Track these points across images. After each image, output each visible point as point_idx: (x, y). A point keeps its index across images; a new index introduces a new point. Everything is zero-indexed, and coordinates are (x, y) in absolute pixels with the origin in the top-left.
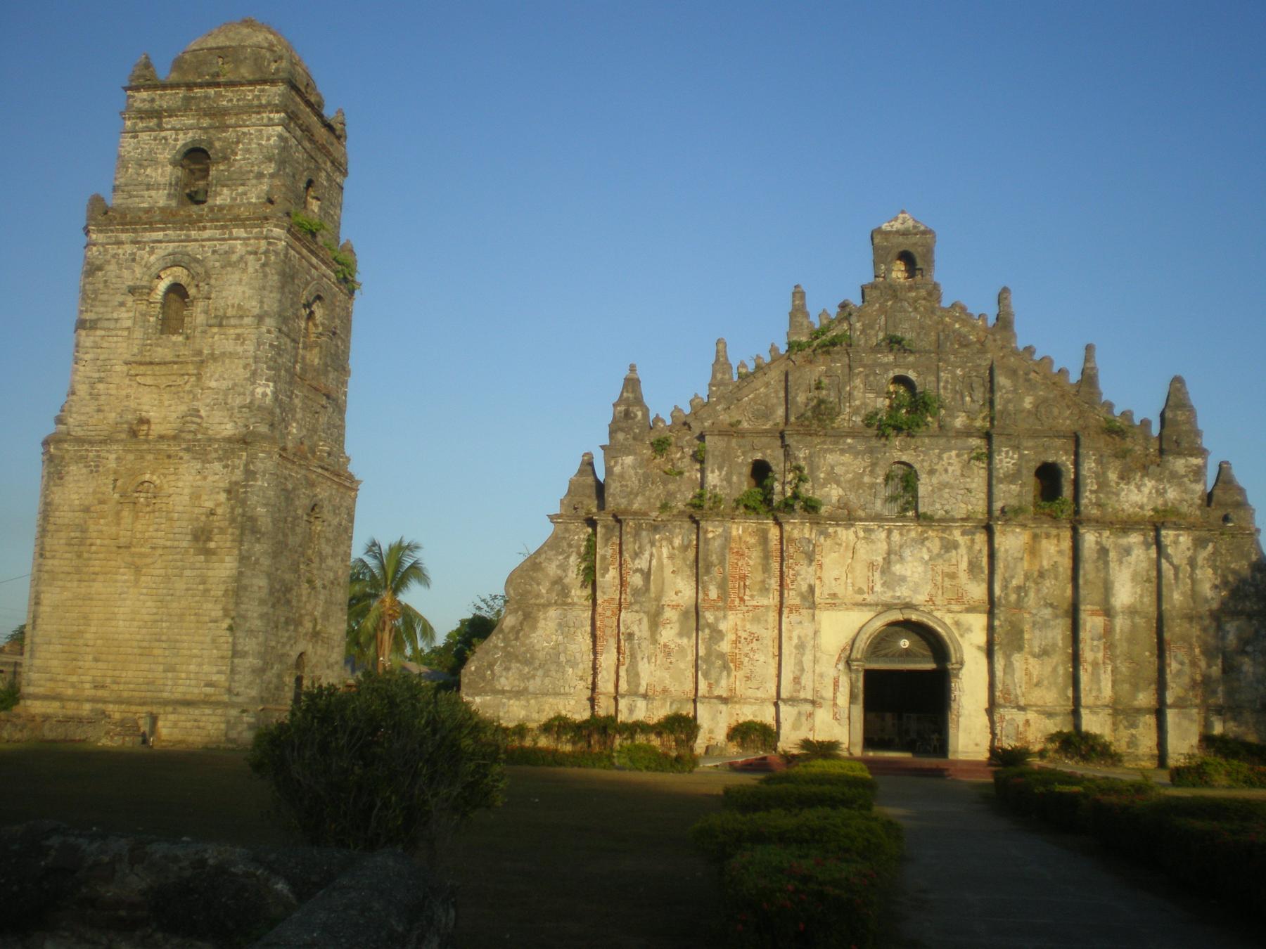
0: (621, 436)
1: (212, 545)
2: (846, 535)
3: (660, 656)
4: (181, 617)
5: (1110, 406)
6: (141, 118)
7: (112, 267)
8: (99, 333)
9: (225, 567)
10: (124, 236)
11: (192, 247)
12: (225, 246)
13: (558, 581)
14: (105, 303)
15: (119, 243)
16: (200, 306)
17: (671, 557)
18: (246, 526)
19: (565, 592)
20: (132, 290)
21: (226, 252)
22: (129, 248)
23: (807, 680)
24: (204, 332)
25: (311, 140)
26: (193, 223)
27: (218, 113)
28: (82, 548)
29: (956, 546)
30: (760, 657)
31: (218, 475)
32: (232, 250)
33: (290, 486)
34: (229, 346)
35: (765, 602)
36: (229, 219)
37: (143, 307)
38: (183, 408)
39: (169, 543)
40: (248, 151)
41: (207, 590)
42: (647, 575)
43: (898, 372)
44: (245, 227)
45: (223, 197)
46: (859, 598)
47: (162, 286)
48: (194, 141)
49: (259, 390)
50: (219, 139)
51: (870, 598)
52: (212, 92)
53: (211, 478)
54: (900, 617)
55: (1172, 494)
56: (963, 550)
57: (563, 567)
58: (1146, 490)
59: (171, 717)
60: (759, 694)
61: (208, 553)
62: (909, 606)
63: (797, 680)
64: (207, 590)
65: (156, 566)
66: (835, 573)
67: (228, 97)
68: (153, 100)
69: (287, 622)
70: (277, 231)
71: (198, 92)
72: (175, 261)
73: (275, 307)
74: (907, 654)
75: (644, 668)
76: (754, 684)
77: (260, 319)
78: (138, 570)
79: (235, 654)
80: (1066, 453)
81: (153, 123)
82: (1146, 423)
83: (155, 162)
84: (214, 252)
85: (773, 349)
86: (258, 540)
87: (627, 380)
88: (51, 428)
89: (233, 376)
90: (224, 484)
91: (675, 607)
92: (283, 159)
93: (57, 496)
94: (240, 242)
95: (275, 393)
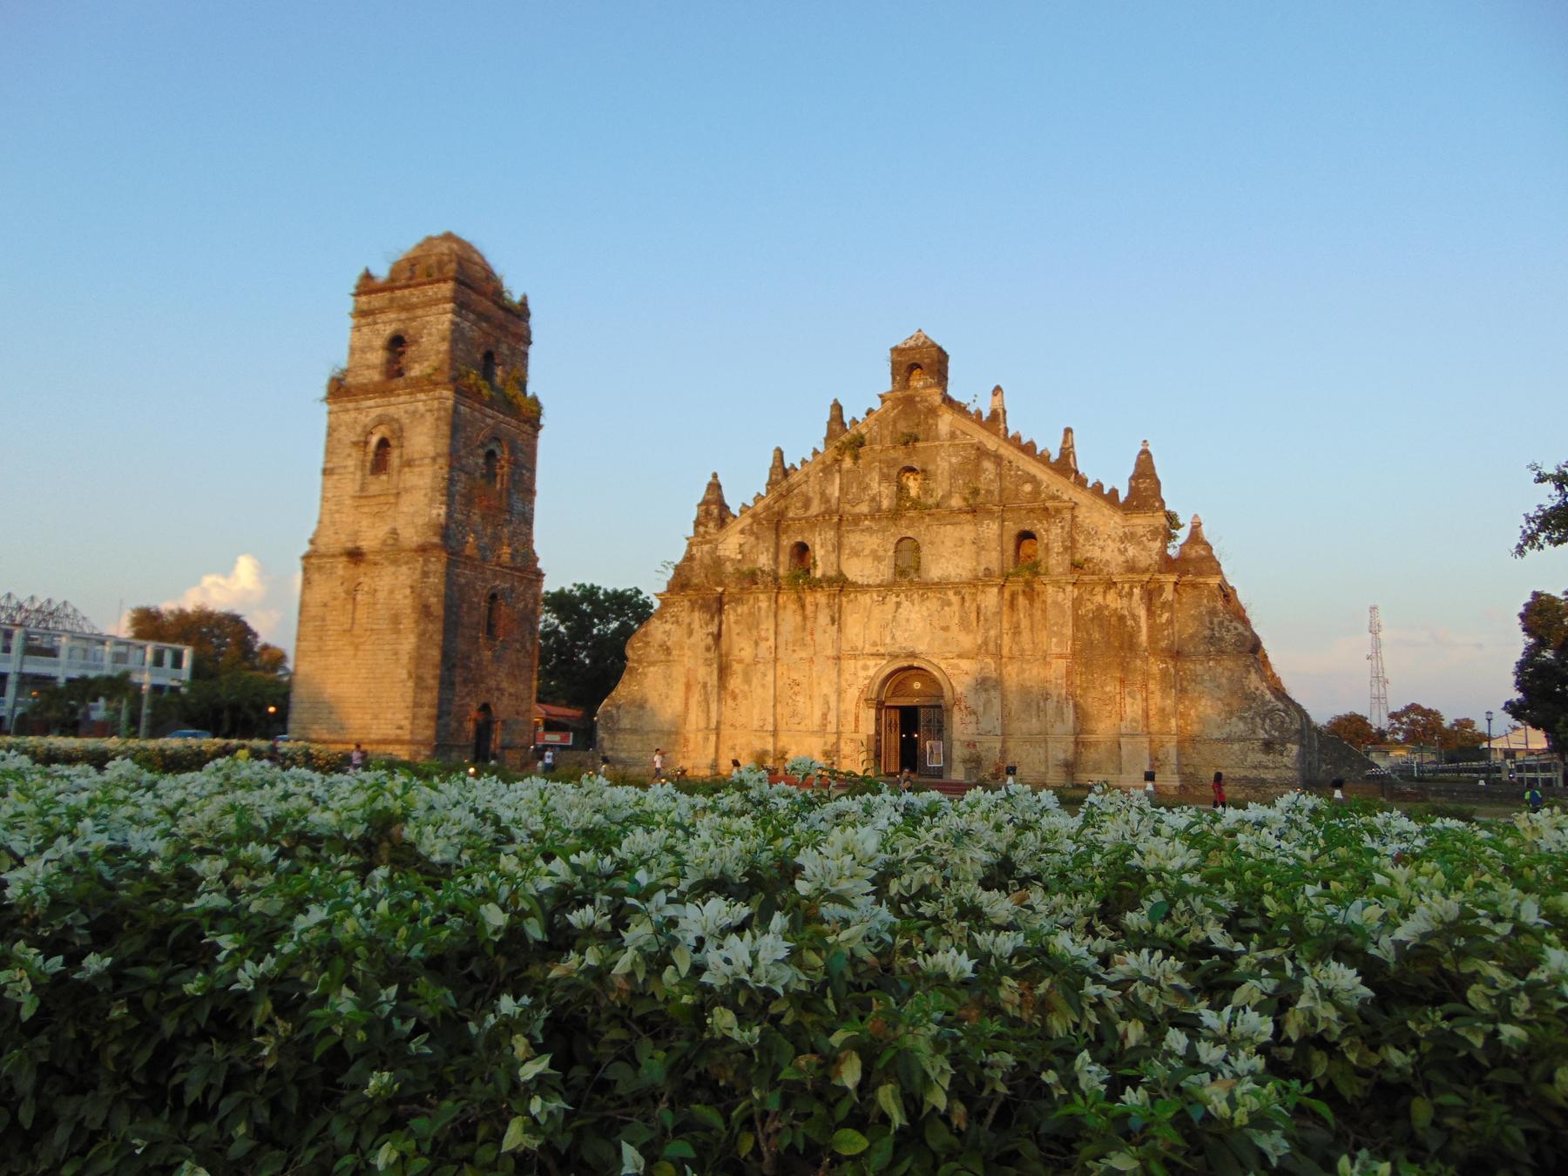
0: (702, 529)
2: (865, 599)
3: (730, 702)
5: (1081, 482)
7: (343, 428)
9: (408, 643)
10: (350, 406)
11: (392, 410)
12: (411, 408)
15: (347, 411)
17: (736, 622)
18: (425, 611)
19: (668, 651)
20: (355, 444)
21: (414, 412)
22: (353, 414)
23: (832, 717)
25: (487, 319)
27: (408, 307)
29: (949, 604)
30: (800, 698)
35: (804, 655)
36: (417, 385)
38: (387, 528)
40: (430, 334)
42: (718, 637)
43: (907, 463)
44: (422, 391)
45: (416, 371)
46: (874, 650)
47: (374, 440)
48: (397, 331)
49: (435, 512)
51: (882, 650)
52: (406, 292)
54: (905, 664)
55: (1132, 551)
56: (956, 607)
58: (1109, 550)
60: (801, 727)
61: (397, 631)
62: (913, 655)
63: (825, 716)
66: (856, 630)
67: (414, 296)
70: (446, 393)
71: (398, 293)
73: (446, 450)
74: (918, 694)
75: (714, 707)
76: (797, 720)
77: (434, 459)
78: (357, 648)
79: (417, 704)
80: (1040, 521)
81: (370, 319)
82: (1114, 492)
83: (371, 348)
85: (816, 453)
87: (710, 485)
88: (306, 548)
89: (418, 503)
90: (409, 582)
91: (740, 661)
92: (457, 335)
93: (308, 597)
94: (422, 402)
95: (449, 515)
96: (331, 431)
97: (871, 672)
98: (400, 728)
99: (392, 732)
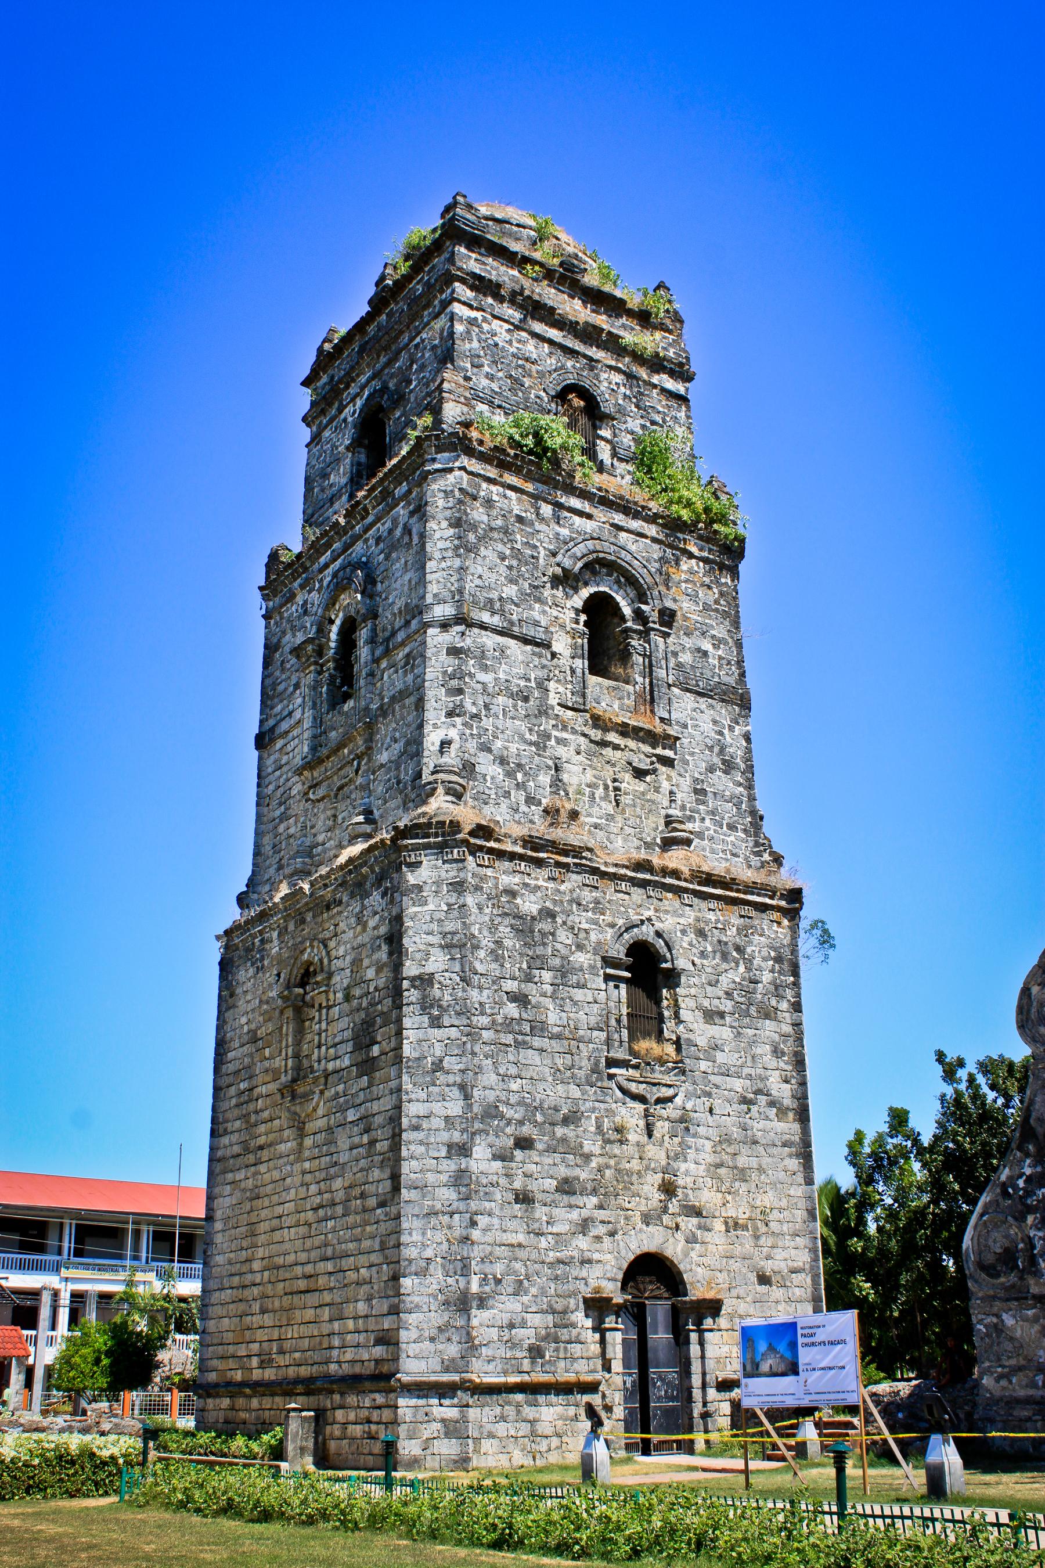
1: (376, 1050)
6: (323, 412)
8: (279, 744)
24: (371, 674)
28: (251, 1107)
33: (529, 905)
39: (331, 1066)
41: (372, 1143)
50: (392, 376)
53: (372, 923)
59: (339, 1414)
64: (372, 1143)
65: (320, 1112)
68: (332, 377)
69: (567, 1187)
84: (378, 540)
86: (436, 1023)
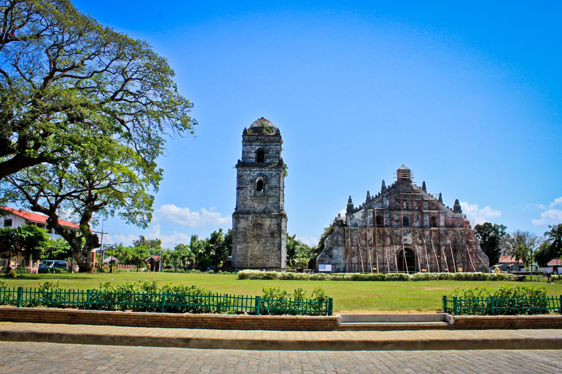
4: (269, 251)
11: (263, 172)
13: (337, 240)
14: (244, 184)
15: (246, 171)
16: (267, 185)
22: (249, 172)
26: (264, 167)
31: (274, 221)
32: (272, 173)
34: (273, 194)
37: (253, 185)
47: (257, 181)
57: (338, 238)
61: (274, 237)
62: (408, 245)
72: (260, 175)
78: (258, 241)
83: (251, 153)
96: (239, 177)
97: (398, 249)
98: (276, 264)
99: (274, 265)
